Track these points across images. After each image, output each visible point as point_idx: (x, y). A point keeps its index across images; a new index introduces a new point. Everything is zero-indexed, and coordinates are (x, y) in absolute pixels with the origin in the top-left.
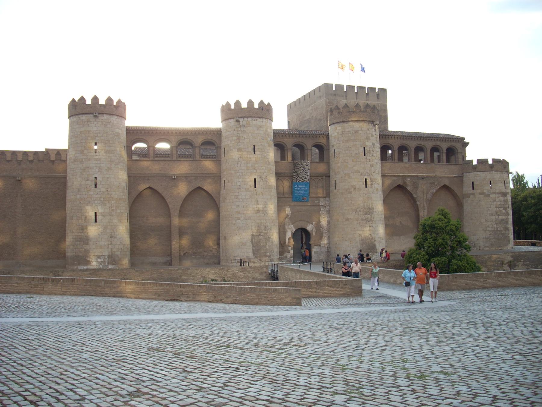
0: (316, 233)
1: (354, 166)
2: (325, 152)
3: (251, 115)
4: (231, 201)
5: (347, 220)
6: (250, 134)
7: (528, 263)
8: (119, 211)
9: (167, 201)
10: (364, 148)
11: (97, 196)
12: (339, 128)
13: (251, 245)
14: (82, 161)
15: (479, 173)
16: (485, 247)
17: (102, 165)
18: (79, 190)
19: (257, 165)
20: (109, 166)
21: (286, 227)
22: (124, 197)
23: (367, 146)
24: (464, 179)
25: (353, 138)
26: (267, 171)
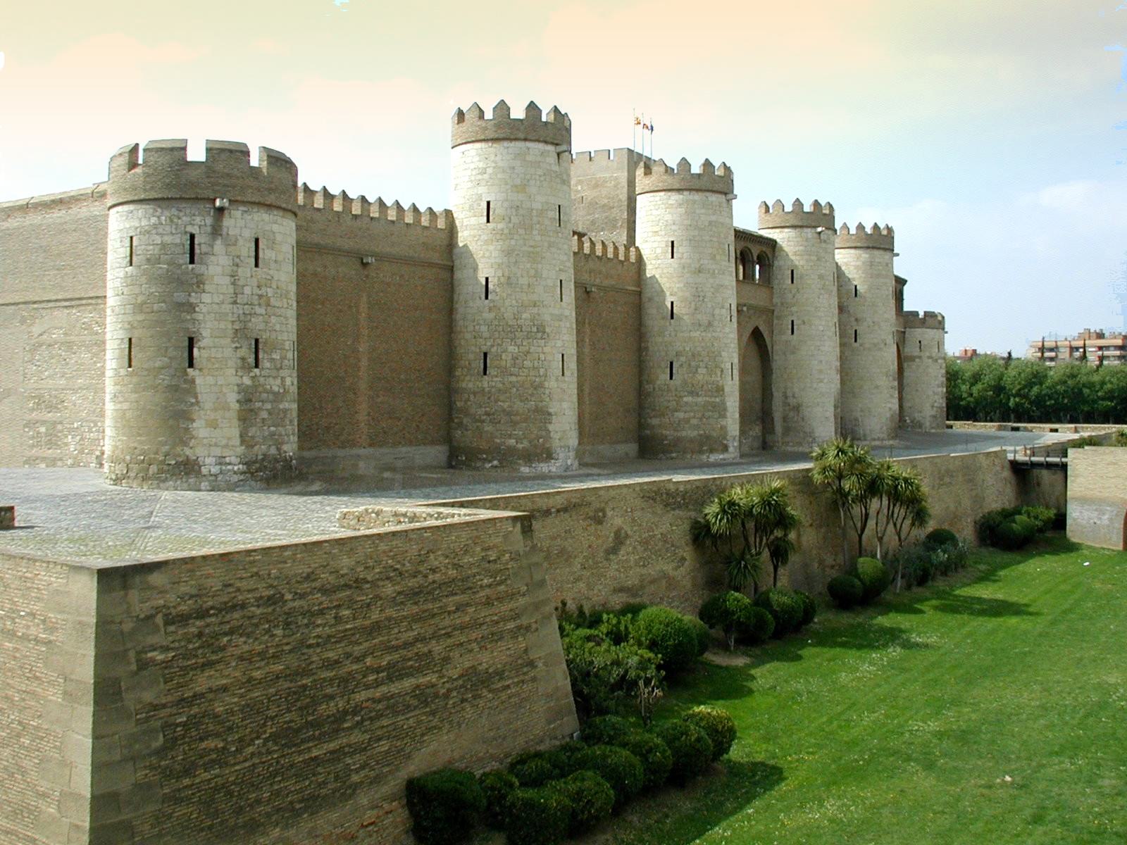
5: (877, 387)
14: (714, 273)
15: (928, 330)
16: (933, 428)
24: (907, 335)
25: (884, 272)
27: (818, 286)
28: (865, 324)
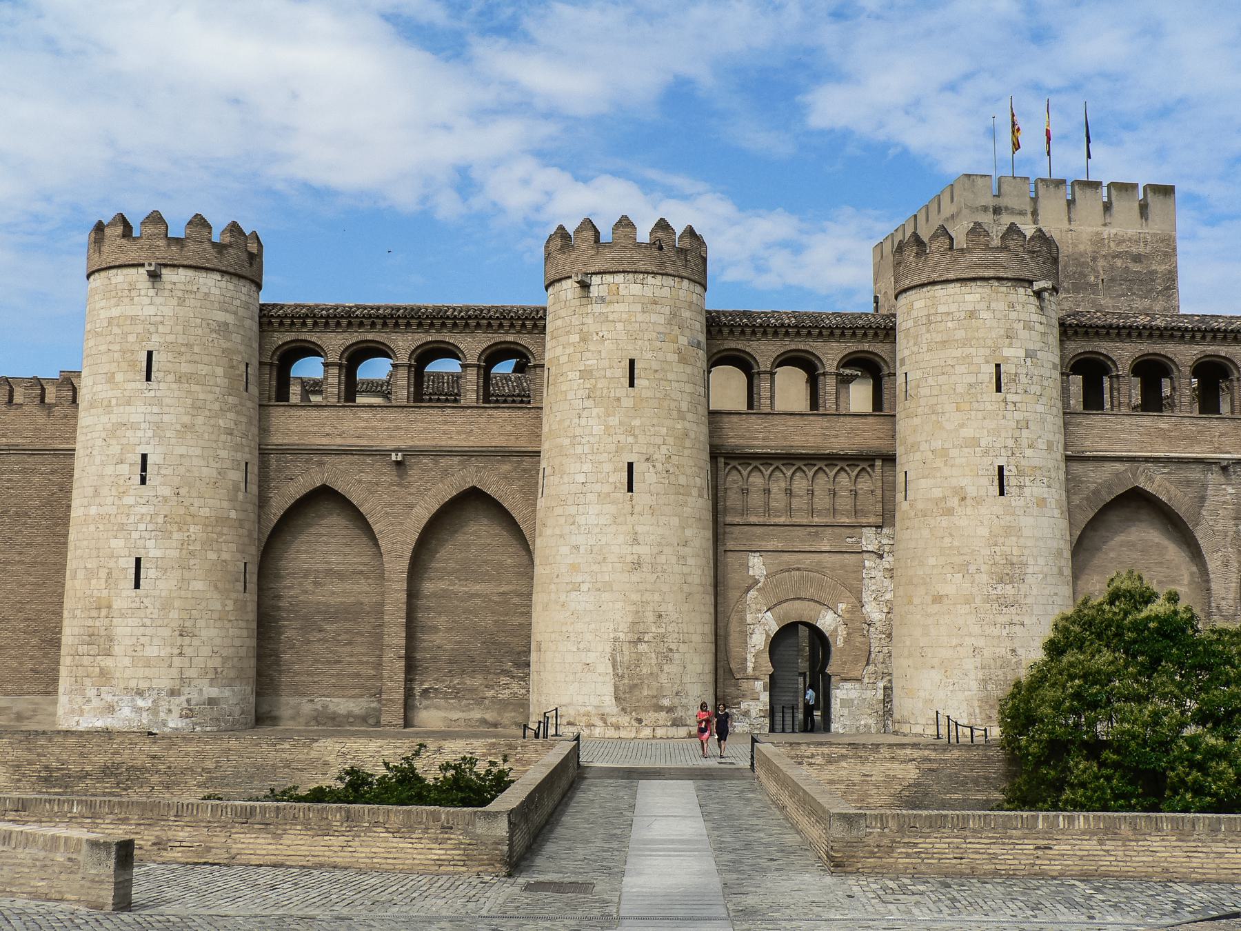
0: (847, 641)
1: (962, 426)
2: (886, 384)
3: (626, 267)
4: (557, 531)
5: (938, 599)
6: (620, 326)
8: (212, 556)
9: (376, 528)
10: (998, 366)
11: (144, 510)
12: (917, 305)
13: (610, 670)
17: (166, 418)
18: (96, 492)
19: (636, 422)
20: (186, 419)
21: (749, 618)
22: (233, 514)
23: (1007, 358)
25: (960, 334)
26: (670, 440)
27: (581, 393)
28: (918, 456)
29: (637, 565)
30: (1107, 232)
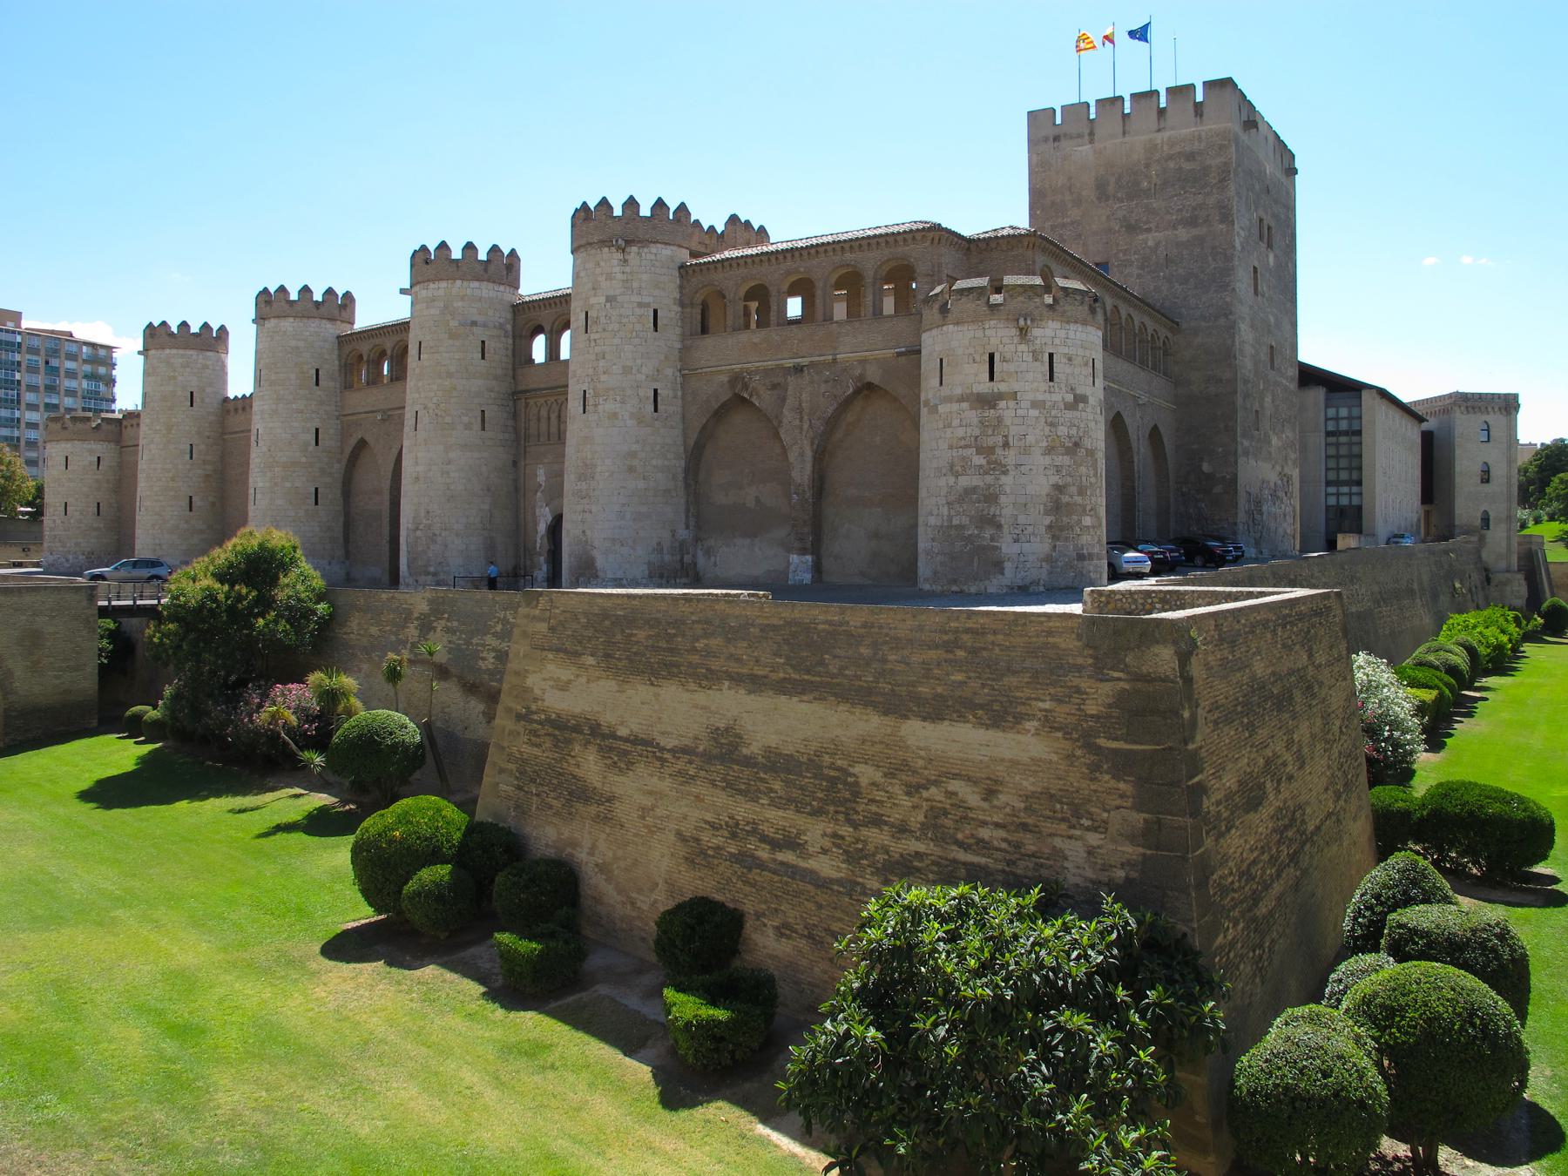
7: (455, 624)
8: (288, 485)
22: (304, 460)
29: (417, 478)
30: (1159, 137)
